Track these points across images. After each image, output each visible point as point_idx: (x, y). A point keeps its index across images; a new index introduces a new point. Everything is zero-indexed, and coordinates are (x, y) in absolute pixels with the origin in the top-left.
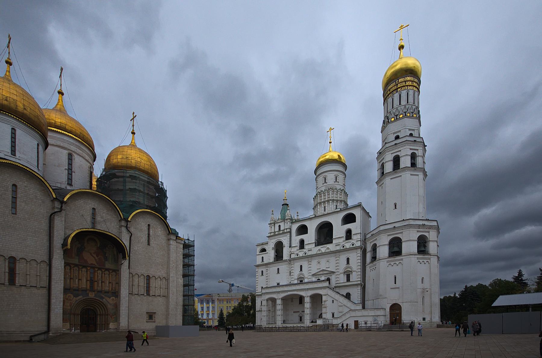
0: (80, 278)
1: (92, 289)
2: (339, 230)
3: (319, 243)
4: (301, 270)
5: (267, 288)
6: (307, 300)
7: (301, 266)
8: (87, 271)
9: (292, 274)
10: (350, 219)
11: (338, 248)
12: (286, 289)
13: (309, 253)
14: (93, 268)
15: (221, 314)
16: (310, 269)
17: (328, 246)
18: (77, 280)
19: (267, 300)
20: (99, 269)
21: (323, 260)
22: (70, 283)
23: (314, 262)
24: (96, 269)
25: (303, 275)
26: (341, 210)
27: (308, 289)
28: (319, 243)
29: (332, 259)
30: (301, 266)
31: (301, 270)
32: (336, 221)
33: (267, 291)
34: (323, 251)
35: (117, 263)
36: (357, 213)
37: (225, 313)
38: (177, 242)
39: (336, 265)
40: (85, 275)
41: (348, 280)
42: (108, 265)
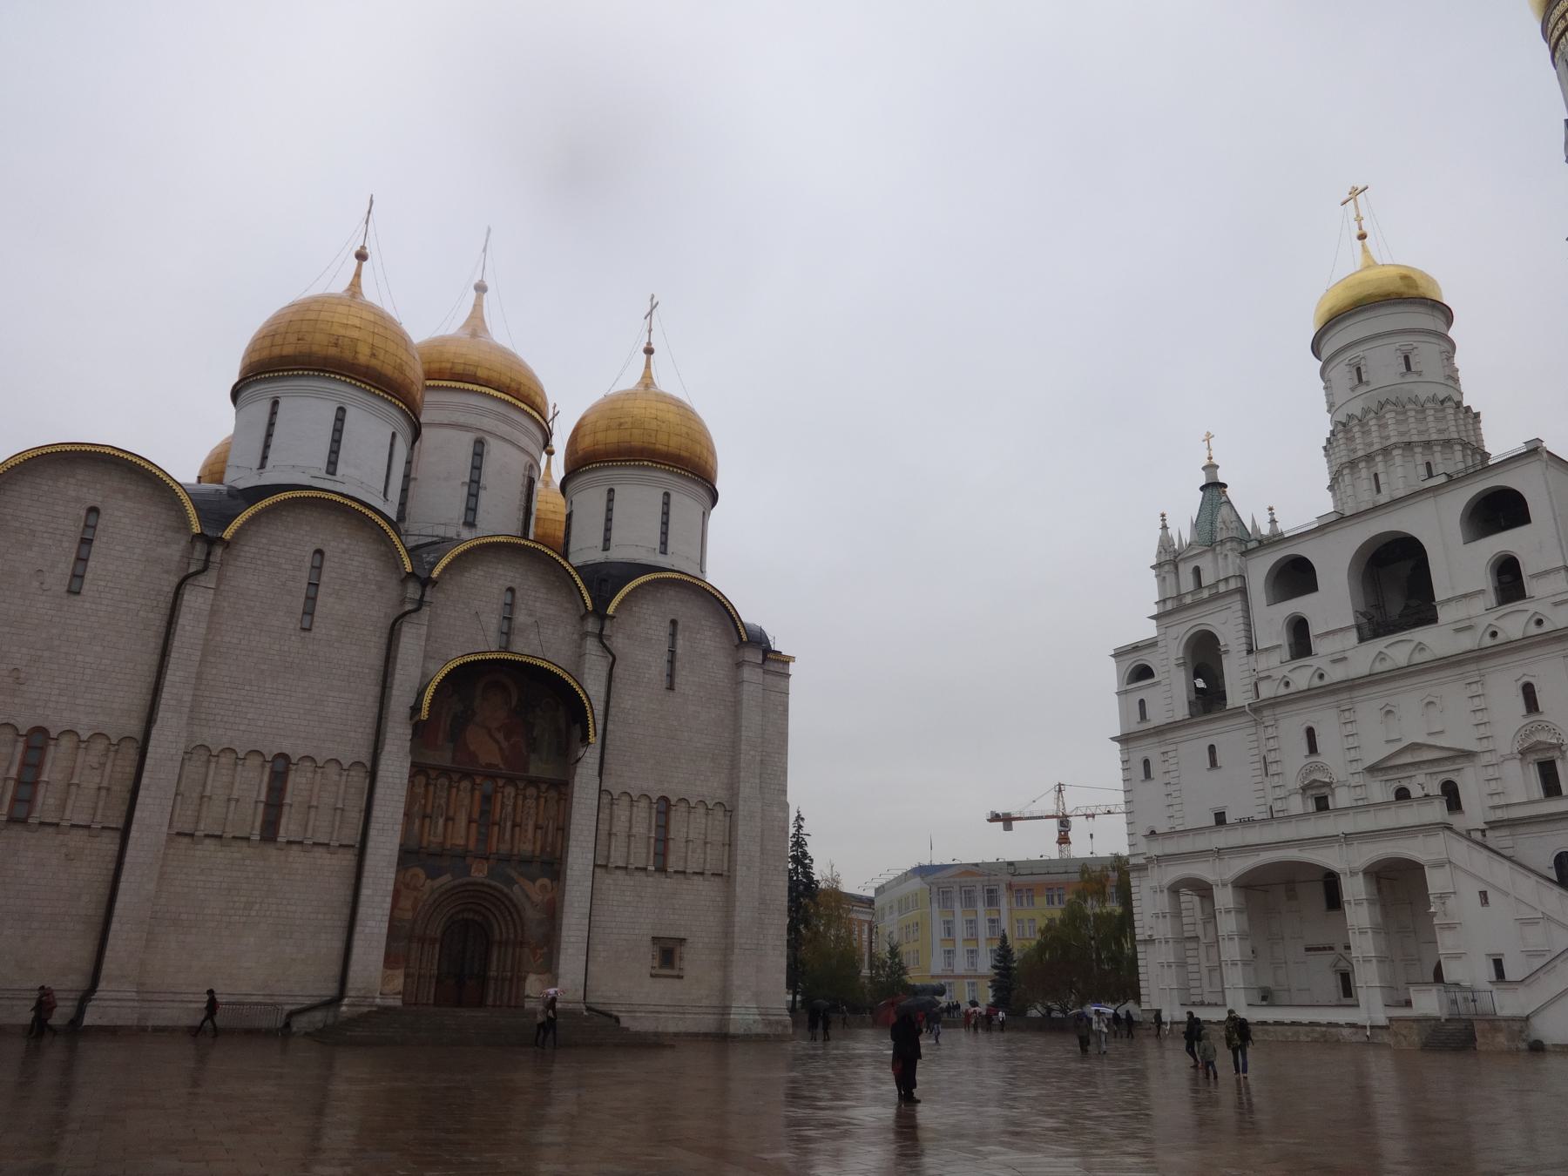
0: (451, 813)
4: (1313, 748)
5: (1172, 834)
7: (1310, 733)
8: (473, 790)
9: (1273, 769)
11: (1467, 642)
12: (1252, 836)
15: (1004, 953)
16: (1358, 739)
18: (441, 821)
19: (1175, 889)
20: (511, 780)
21: (1408, 699)
22: (422, 834)
23: (1368, 708)
24: (500, 783)
25: (1322, 769)
30: (1310, 733)
31: (1313, 748)
33: (1171, 847)
34: (1403, 662)
35: (567, 758)
37: (1016, 947)
38: (766, 672)
40: (467, 802)
42: (538, 767)
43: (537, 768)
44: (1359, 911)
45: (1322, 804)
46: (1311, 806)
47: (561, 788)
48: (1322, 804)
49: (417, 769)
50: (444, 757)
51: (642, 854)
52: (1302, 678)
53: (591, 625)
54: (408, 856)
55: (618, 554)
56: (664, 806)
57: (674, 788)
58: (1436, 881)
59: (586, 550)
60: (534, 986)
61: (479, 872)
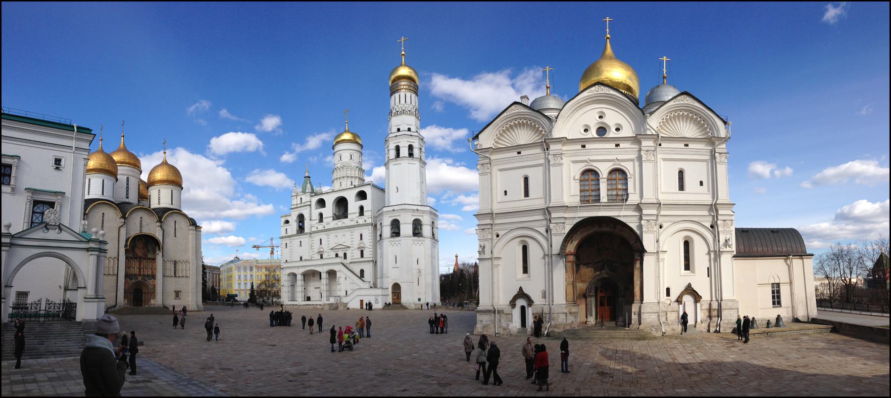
1: (140, 275)
2: (353, 206)
3: (336, 217)
6: (324, 275)
10: (362, 195)
13: (327, 227)
14: (140, 258)
17: (344, 220)
21: (340, 233)
26: (355, 187)
27: (323, 265)
28: (336, 217)
29: (347, 233)
32: (351, 196)
36: (368, 190)
39: (349, 238)
41: (362, 256)
43: (150, 256)
44: (324, 281)
45: (322, 257)
46: (319, 257)
47: (154, 259)
48: (322, 257)
49: (127, 258)
50: (131, 255)
51: (173, 274)
52: (320, 227)
53: (158, 224)
54: (127, 276)
55: (162, 205)
56: (175, 263)
57: (177, 259)
58: (338, 274)
59: (154, 204)
60: (152, 302)
61: (140, 279)
